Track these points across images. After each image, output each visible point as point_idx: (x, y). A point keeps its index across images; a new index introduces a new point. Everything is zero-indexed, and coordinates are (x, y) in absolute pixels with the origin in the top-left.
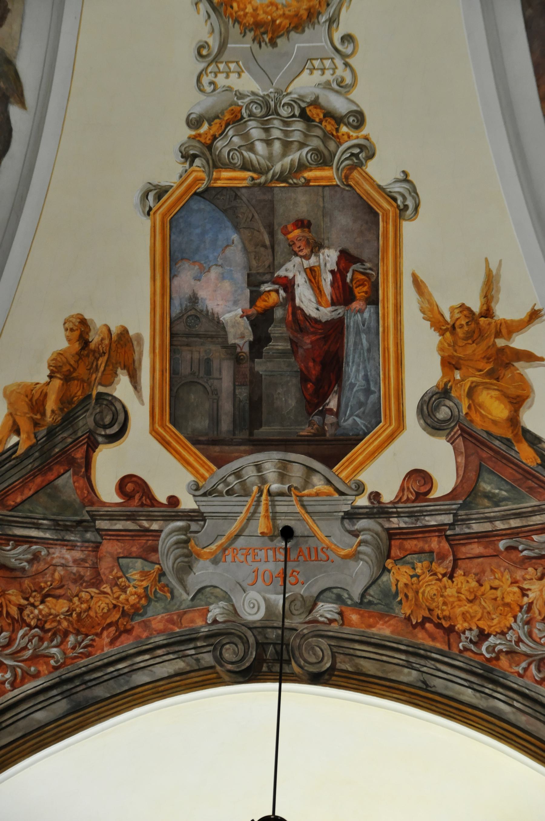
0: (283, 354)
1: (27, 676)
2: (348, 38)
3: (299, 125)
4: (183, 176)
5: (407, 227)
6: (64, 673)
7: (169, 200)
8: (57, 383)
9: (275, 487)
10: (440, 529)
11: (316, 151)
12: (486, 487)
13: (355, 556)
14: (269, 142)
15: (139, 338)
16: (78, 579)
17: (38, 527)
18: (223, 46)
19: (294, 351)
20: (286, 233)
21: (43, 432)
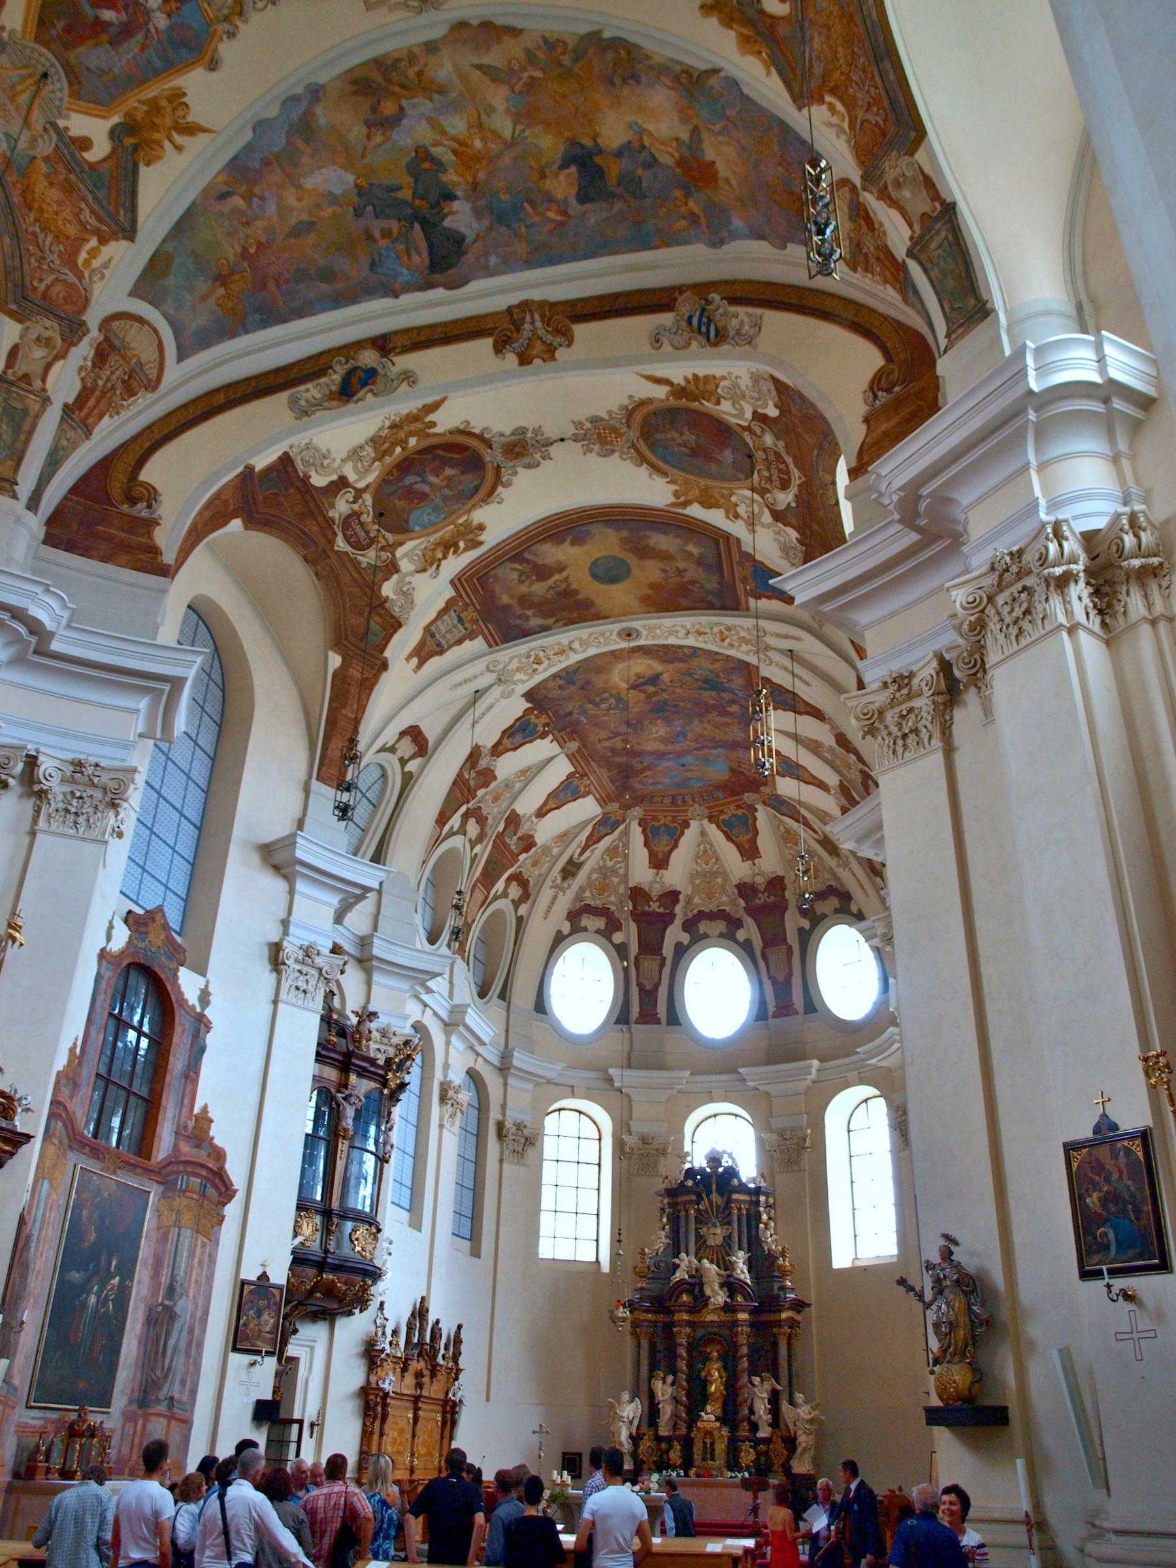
1: (872, 78)
6: (872, 59)
16: (828, 37)
17: (804, 53)
21: (759, 39)
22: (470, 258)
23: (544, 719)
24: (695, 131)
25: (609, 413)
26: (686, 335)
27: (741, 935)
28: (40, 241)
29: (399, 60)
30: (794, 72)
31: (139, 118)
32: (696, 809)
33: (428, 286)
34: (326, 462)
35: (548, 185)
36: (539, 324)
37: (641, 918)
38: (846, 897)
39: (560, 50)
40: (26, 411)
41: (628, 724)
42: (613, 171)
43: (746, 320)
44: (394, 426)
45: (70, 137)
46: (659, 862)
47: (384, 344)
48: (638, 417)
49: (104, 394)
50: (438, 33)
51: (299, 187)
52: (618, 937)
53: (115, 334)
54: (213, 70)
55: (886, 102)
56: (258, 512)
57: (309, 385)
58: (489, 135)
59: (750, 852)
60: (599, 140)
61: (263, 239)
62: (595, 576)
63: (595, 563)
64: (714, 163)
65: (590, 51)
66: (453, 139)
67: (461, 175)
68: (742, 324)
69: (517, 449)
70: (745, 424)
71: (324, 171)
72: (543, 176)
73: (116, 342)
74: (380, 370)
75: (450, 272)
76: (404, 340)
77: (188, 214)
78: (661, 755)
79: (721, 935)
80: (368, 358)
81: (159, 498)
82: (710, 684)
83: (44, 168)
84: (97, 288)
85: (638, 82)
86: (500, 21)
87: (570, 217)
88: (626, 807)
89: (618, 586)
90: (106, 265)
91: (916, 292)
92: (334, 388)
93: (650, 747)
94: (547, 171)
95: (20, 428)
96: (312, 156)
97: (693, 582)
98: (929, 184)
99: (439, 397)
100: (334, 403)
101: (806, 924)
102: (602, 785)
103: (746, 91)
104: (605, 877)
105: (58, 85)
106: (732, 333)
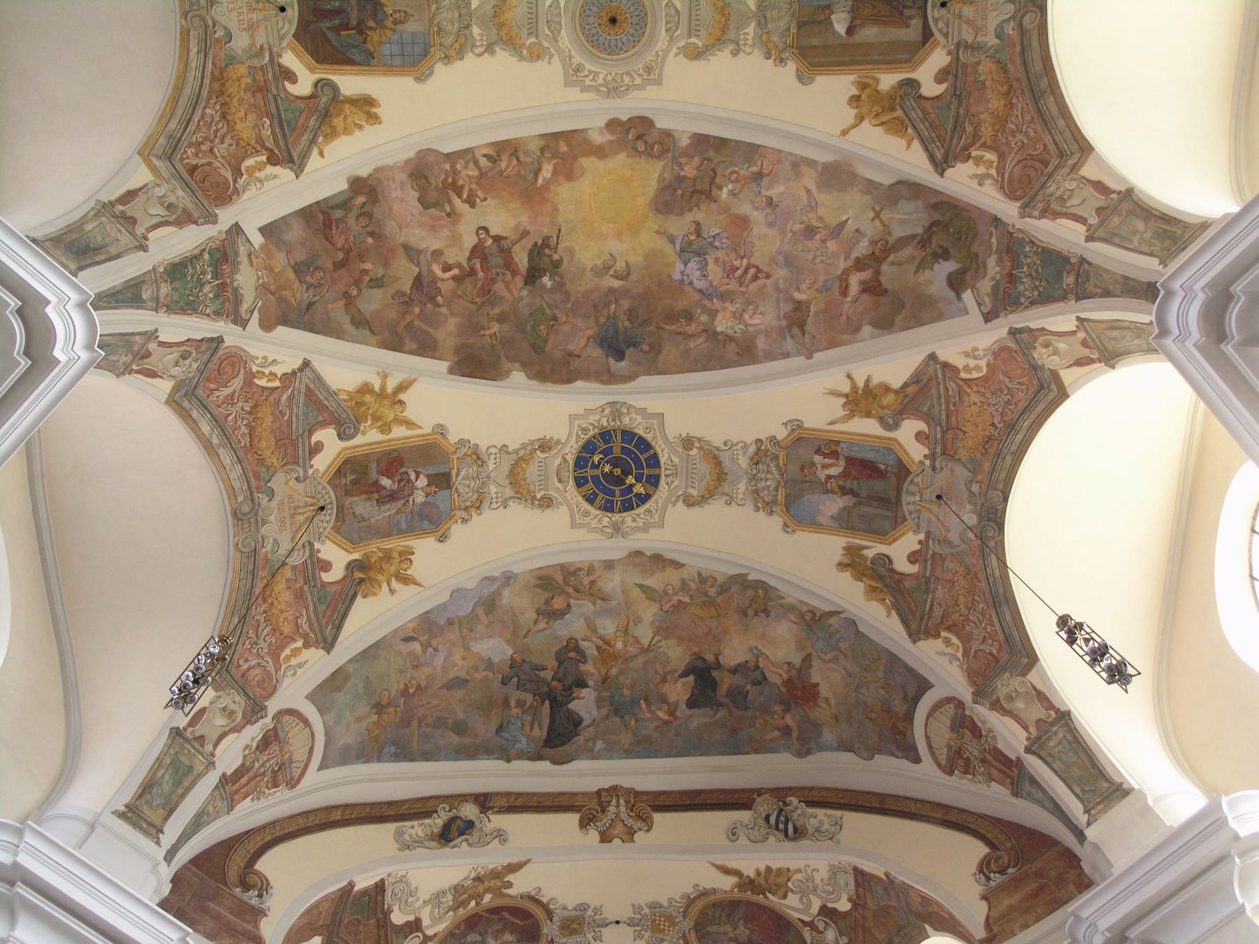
0: (859, 484)
1: (990, 619)
2: (725, 444)
3: (760, 466)
4: (780, 516)
5: (806, 425)
7: (789, 523)
8: (865, 579)
9: (918, 498)
10: (943, 433)
11: (771, 460)
12: (925, 409)
13: (952, 471)
14: (767, 479)
15: (848, 542)
16: (951, 589)
17: (926, 600)
18: (727, 495)
19: (858, 479)
20: (805, 476)
21: (885, 589)
22: (579, 740)
24: (808, 659)
25: (670, 900)
26: (763, 831)
28: (260, 629)
29: (580, 569)
30: (914, 613)
31: (373, 560)
33: (539, 757)
34: (411, 900)
36: (622, 809)
39: (709, 584)
40: (191, 768)
42: (726, 682)
43: (826, 820)
44: (478, 879)
45: (318, 558)
47: (484, 801)
48: (698, 906)
49: (255, 776)
50: (616, 556)
51: (467, 648)
53: (283, 727)
54: (441, 541)
55: (1001, 636)
56: (338, 936)
57: (415, 823)
58: (631, 640)
60: (720, 658)
61: (423, 684)
64: (817, 685)
65: (734, 589)
66: (601, 638)
67: (597, 668)
68: (821, 823)
69: (574, 926)
70: (807, 919)
71: (491, 641)
72: (664, 680)
73: (281, 735)
74: (477, 823)
75: (561, 748)
76: (502, 802)
77: (376, 646)
80: (469, 811)
81: (271, 891)
83: (288, 573)
84: (287, 682)
85: (768, 616)
86: (668, 555)
87: (676, 718)
90: (300, 666)
91: (1033, 782)
92: (436, 831)
94: (669, 677)
95: (180, 782)
96: (487, 626)
98: (1042, 697)
99: (524, 859)
100: (434, 844)
103: (861, 629)
105: (328, 518)
106: (811, 830)
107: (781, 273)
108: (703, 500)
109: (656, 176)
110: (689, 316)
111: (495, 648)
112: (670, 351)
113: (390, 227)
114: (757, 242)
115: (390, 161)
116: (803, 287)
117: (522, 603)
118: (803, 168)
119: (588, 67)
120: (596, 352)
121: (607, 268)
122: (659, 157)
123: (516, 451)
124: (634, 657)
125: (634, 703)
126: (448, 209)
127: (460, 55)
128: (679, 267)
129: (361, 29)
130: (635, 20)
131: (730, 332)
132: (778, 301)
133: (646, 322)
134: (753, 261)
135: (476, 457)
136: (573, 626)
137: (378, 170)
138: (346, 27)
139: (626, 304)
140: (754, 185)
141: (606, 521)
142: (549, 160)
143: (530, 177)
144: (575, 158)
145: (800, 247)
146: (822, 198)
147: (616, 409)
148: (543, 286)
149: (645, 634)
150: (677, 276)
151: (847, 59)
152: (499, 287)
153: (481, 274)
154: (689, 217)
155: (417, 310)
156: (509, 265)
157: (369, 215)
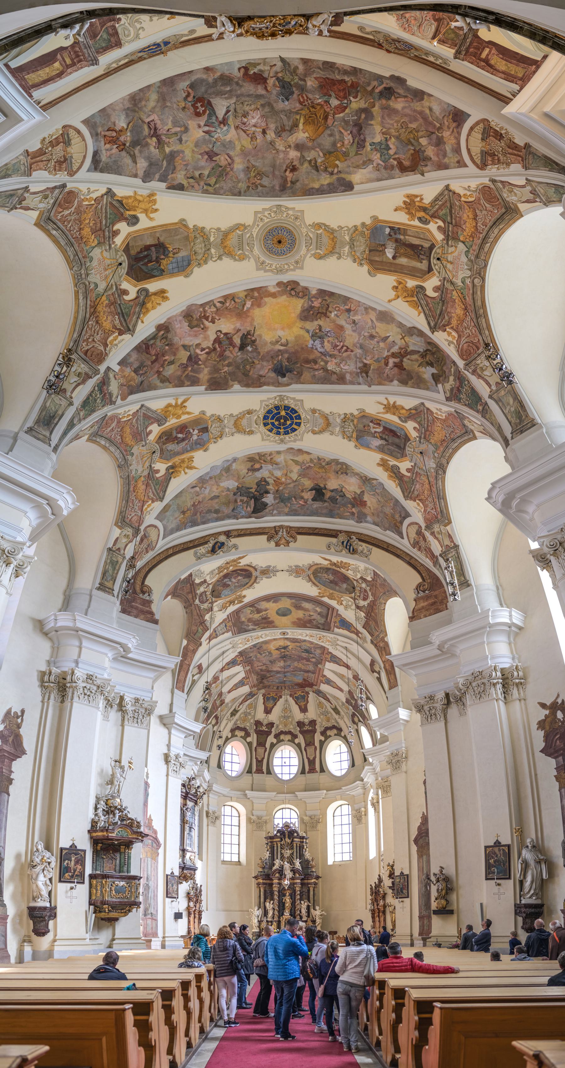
22: (267, 510)
23: (241, 659)
27: (297, 741)
32: (287, 692)
33: (250, 517)
35: (303, 494)
37: (258, 732)
38: (340, 730)
41: (270, 661)
42: (328, 495)
46: (268, 711)
48: (314, 568)
50: (282, 449)
52: (249, 739)
59: (304, 710)
62: (277, 613)
63: (279, 609)
72: (302, 491)
76: (236, 533)
78: (278, 672)
79: (289, 741)
82: (307, 651)
88: (259, 689)
89: (285, 618)
93: (275, 669)
97: (314, 620)
101: (323, 739)
102: (253, 681)
104: (246, 716)
107: (359, 351)
108: (320, 432)
109: (300, 305)
110: (315, 362)
111: (232, 484)
112: (307, 375)
113: (176, 340)
114: (347, 337)
115: (174, 314)
116: (368, 358)
117: (243, 469)
118: (370, 310)
119: (267, 262)
120: (273, 375)
121: (277, 342)
122: (302, 298)
123: (237, 415)
124: (290, 484)
125: (289, 499)
126: (202, 326)
127: (206, 262)
128: (311, 342)
129: (158, 261)
130: (290, 241)
131: (334, 370)
132: (356, 361)
133: (296, 363)
134: (345, 344)
135: (219, 419)
136: (264, 473)
137: (168, 319)
138: (150, 261)
139: (286, 356)
140: (347, 314)
141: (277, 438)
142: (249, 300)
143: (241, 308)
144: (262, 298)
145: (367, 342)
146: (378, 324)
147: (282, 398)
148: (248, 351)
149: (294, 476)
150: (310, 346)
151: (392, 269)
152: (227, 353)
153: (219, 349)
154: (316, 323)
155: (190, 369)
156: (232, 344)
157: (166, 338)
